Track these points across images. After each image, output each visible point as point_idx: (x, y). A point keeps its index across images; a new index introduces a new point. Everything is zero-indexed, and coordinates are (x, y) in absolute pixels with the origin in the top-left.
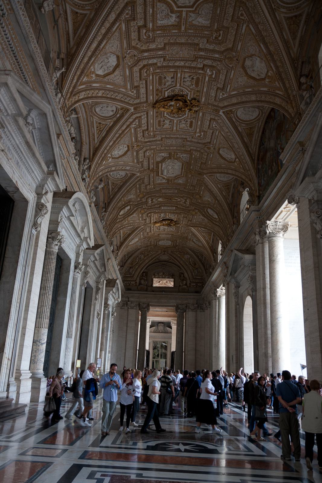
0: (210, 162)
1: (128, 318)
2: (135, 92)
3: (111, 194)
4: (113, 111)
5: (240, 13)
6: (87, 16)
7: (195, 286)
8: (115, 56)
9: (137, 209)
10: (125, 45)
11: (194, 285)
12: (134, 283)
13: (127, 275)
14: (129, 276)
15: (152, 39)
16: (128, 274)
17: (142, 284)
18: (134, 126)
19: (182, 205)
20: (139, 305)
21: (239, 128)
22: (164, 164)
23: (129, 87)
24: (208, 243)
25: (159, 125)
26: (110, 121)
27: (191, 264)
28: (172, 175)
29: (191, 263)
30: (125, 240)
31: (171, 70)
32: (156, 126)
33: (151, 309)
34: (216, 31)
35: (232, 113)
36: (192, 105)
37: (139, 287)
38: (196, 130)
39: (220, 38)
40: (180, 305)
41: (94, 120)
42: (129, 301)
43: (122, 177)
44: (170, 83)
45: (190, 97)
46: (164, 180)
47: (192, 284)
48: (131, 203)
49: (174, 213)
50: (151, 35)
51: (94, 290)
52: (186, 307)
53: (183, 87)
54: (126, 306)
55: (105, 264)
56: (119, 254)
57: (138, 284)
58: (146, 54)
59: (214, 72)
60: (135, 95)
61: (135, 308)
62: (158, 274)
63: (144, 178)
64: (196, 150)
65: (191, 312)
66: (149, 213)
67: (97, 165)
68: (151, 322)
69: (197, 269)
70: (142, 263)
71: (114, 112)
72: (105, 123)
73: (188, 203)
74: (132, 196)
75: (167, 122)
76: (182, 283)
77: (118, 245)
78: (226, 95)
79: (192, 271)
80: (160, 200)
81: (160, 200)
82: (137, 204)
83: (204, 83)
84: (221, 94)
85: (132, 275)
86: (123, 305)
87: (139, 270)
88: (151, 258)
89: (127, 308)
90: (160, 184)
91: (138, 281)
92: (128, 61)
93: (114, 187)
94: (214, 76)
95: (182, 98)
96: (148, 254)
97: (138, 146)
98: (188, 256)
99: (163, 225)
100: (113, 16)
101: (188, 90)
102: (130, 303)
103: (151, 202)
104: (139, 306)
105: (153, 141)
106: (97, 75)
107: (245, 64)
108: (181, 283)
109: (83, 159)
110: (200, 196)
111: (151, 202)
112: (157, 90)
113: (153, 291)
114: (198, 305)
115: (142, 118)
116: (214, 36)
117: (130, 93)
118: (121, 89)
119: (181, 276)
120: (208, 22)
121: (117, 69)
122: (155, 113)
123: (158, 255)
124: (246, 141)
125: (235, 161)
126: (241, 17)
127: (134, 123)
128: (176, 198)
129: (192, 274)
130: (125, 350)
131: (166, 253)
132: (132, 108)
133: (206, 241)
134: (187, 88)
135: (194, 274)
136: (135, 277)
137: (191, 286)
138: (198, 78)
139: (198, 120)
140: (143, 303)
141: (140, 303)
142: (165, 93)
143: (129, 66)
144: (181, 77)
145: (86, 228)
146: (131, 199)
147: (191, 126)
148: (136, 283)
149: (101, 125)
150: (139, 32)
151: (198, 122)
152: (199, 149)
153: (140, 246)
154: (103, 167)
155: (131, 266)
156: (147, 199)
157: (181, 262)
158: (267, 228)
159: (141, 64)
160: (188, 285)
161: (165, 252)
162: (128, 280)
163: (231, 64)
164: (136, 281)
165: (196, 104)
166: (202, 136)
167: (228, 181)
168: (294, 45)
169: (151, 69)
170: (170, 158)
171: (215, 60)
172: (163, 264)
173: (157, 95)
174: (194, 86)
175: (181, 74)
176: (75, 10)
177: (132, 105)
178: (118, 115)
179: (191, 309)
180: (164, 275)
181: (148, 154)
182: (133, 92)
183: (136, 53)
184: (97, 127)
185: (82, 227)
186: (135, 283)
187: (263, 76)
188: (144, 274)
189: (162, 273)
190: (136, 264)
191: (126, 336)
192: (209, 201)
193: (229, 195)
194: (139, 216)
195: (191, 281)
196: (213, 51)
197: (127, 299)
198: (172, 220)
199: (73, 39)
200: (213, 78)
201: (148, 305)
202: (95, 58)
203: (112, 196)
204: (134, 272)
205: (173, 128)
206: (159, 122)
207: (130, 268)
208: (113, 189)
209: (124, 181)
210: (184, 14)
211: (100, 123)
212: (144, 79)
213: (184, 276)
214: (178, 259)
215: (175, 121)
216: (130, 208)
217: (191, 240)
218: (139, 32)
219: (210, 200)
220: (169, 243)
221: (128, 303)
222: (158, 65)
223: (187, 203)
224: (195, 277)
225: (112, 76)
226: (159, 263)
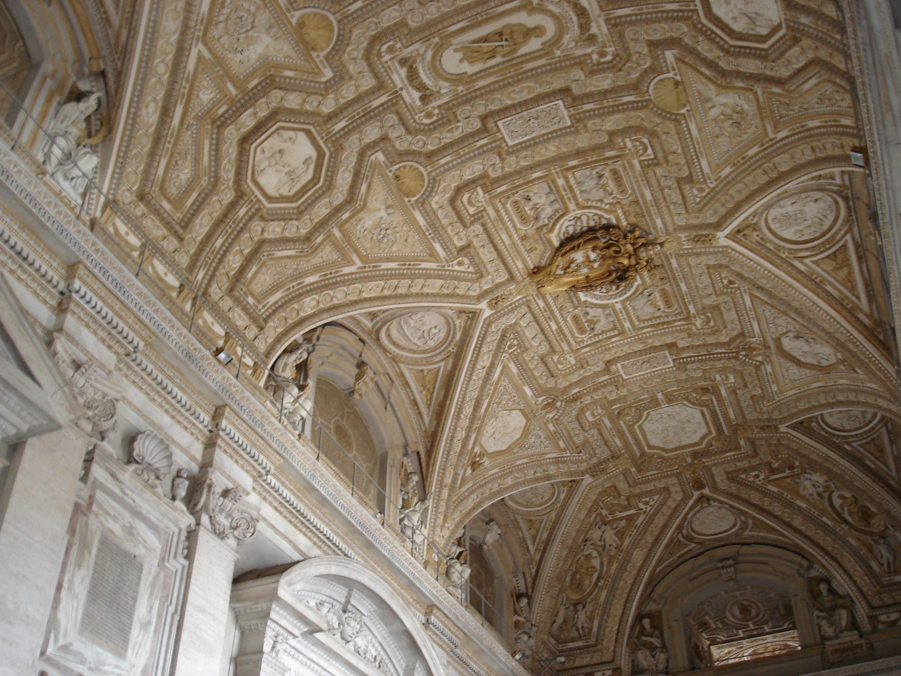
3: (115, 20)
9: (362, 155)
13: (571, 645)
14: (580, 644)
16: (573, 640)
19: (580, 62)
27: (846, 522)
29: (846, 516)
47: (883, 618)
66: (459, 190)
69: (883, 536)
70: (622, 569)
73: (605, 30)
76: (831, 624)
79: (864, 551)
85: (592, 640)
87: (617, 608)
88: (650, 538)
96: (630, 519)
98: (816, 477)
99: (589, 285)
108: (824, 623)
119: (820, 593)
123: (676, 510)
128: (524, 19)
129: (869, 567)
131: (706, 491)
133: (838, 304)
135: (874, 565)
136: (608, 643)
137: (881, 626)
157: (797, 522)
160: (866, 626)
162: (577, 664)
164: (612, 661)
172: (721, 560)
186: (615, 670)
189: (737, 612)
190: (596, 584)
195: (876, 602)
198: (608, 227)
204: (596, 623)
207: (575, 605)
213: (831, 591)
214: (777, 509)
217: (771, 344)
223: (594, 30)
224: (885, 580)
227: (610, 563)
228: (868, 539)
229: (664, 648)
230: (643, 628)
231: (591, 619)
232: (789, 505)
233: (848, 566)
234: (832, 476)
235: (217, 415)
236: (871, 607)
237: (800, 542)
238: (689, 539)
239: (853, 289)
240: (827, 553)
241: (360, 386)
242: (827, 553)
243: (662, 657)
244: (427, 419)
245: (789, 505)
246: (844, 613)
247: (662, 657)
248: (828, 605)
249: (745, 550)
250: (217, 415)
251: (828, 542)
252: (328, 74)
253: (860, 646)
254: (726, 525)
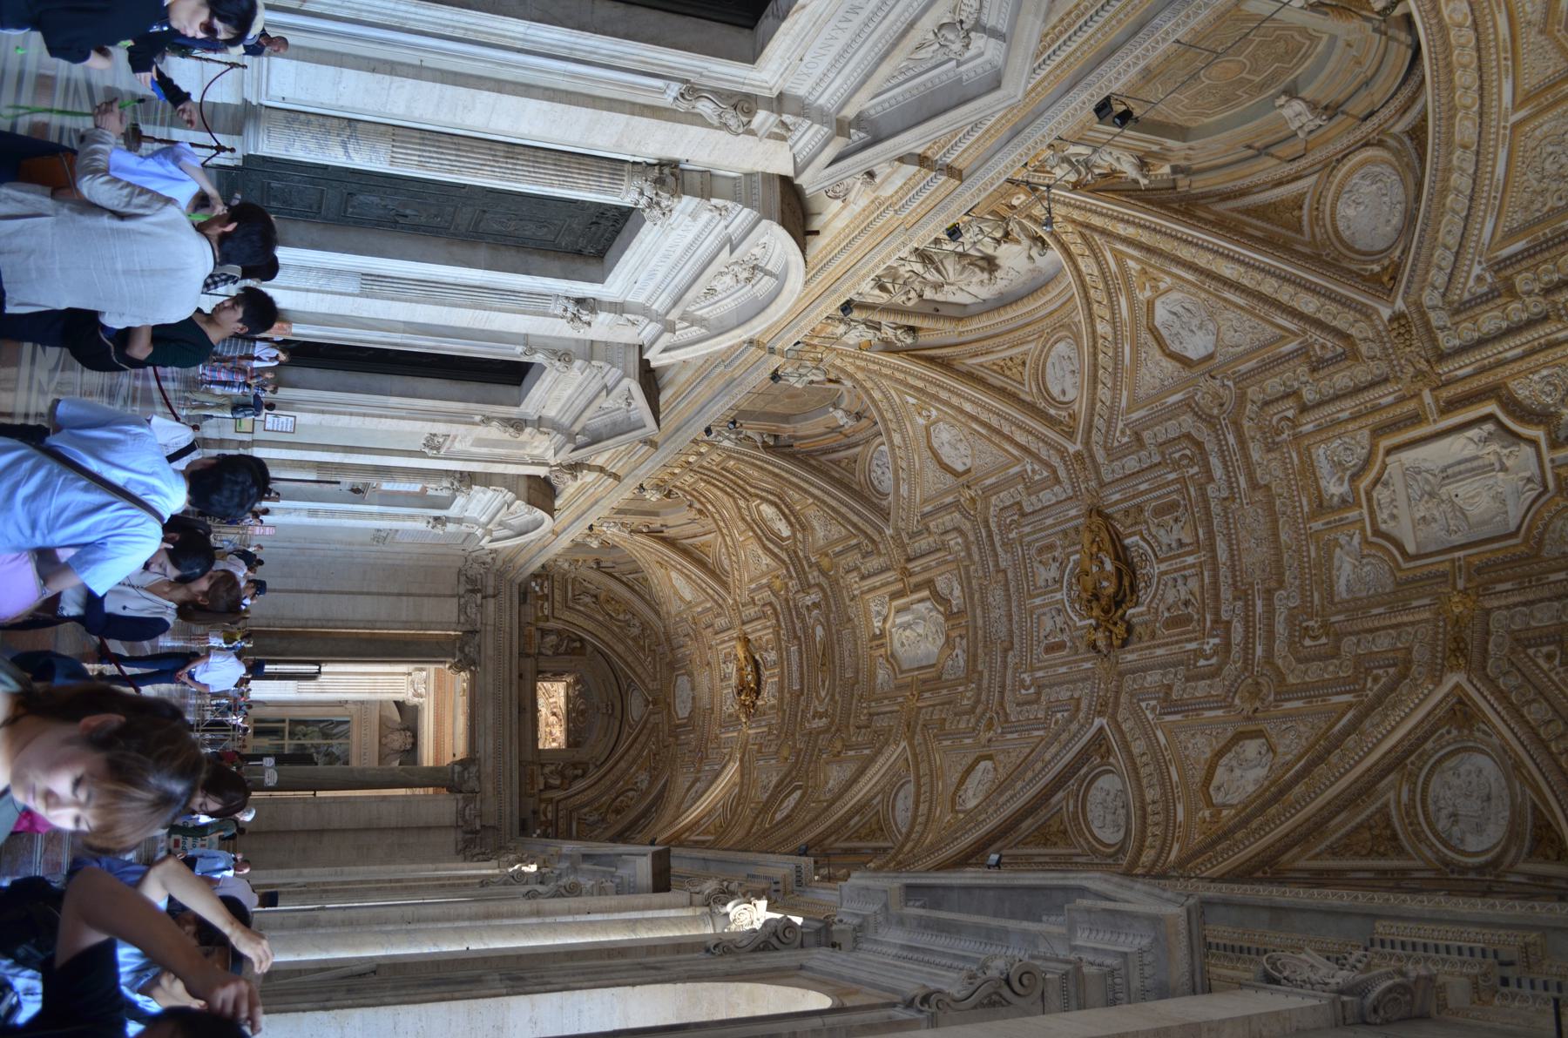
0: (948, 743)
1: (429, 596)
2: (1125, 440)
3: (823, 458)
4: (1064, 392)
5: (1381, 672)
6: (1299, 236)
7: (543, 818)
8: (1211, 349)
9: (783, 562)
10: (1244, 368)
11: (546, 816)
12: (546, 612)
13: (570, 588)
14: (570, 595)
15: (1274, 442)
16: (573, 590)
17: (542, 637)
18: (1029, 468)
20: (474, 632)
21: (1060, 794)
22: (928, 604)
23: (1135, 416)
24: (691, 827)
25: (1040, 551)
26: (1035, 390)
27: (617, 797)
28: (897, 644)
30: (685, 552)
31: (1201, 532)
32: (1037, 540)
33: (461, 680)
34: (1325, 626)
35: (1102, 757)
36: (1111, 627)
37: (533, 629)
38: (1040, 669)
39: (1308, 642)
40: (478, 771)
41: (1032, 345)
43: (876, 483)
44: (1165, 540)
45: (1133, 615)
46: (880, 624)
47: (550, 808)
48: (799, 536)
49: (781, 689)
50: (1284, 436)
51: (513, 412)
52: (473, 791)
53: (1158, 583)
54: (469, 587)
55: (599, 441)
56: (637, 537)
57: (541, 624)
58: (1231, 439)
59: (1214, 660)
60: (1116, 444)
61: (462, 619)
62: (580, 695)
63: (879, 554)
64: (979, 687)
66: (775, 609)
67: (901, 371)
68: (416, 700)
69: (603, 820)
71: (1062, 399)
72: (1026, 378)
74: (820, 533)
75: (1054, 572)
76: (551, 773)
77: (668, 533)
78: (1150, 717)
80: (819, 631)
81: (819, 631)
82: (797, 556)
83: (1177, 642)
84: (1153, 703)
85: (570, 604)
86: (469, 580)
87: (590, 626)
88: (629, 659)
89: (462, 591)
90: (867, 612)
91: (552, 624)
92: (1204, 390)
93: (843, 465)
94: (1202, 662)
95: (1128, 592)
96: (643, 648)
97: (973, 500)
99: (740, 670)
100: (1308, 304)
101: (1151, 602)
102: (479, 602)
103: (809, 603)
104: (471, 632)
105: (992, 544)
106: (1150, 305)
107: (1247, 742)
108: (553, 767)
109: (912, 322)
110: (839, 753)
111: (809, 603)
112: (1140, 509)
113: (521, 676)
114: (477, 832)
115: (1056, 488)
116: (1311, 623)
117: (1120, 425)
118: (1125, 393)
120: (1344, 595)
121: (1178, 365)
122: (1075, 523)
123: (643, 682)
124: (1024, 825)
125: (957, 812)
126: (1370, 679)
127: (1037, 467)
130: (320, 592)
132: (1079, 447)
133: (696, 823)
134: (1158, 597)
135: (587, 809)
136: (567, 615)
137: (543, 806)
138: (1189, 619)
139: (1069, 662)
140: (479, 646)
142: (1134, 534)
143: (1193, 397)
144: (1184, 568)
145: (703, 331)
146: (813, 529)
147: (1051, 649)
148: (547, 619)
149: (1020, 368)
150: (1286, 396)
151: (1063, 664)
152: (983, 697)
153: (668, 613)
154: (897, 400)
155: (602, 597)
156: (818, 585)
157: (623, 764)
158: (742, 900)
159: (1204, 434)
161: (655, 703)
163: (1241, 698)
165: (1114, 637)
166: (1023, 692)
167: (896, 825)
168: (1316, 857)
169: (1196, 469)
170: (949, 616)
171: (1247, 648)
173: (1127, 513)
174: (1166, 614)
175: (1193, 566)
176: (1307, 202)
177: (1087, 443)
178: (1052, 412)
179: (464, 809)
180: (576, 718)
181: (952, 543)
182: (1123, 433)
183: (1228, 407)
184: (1011, 359)
185: (705, 320)
187: (1217, 798)
188: (578, 644)
189: (582, 707)
191: (368, 593)
192: (827, 783)
193: (849, 839)
194: (763, 575)
195: (561, 806)
196: (1270, 635)
197: (490, 591)
198: (758, 693)
199: (1233, 210)
200: (1196, 661)
201: (474, 663)
202: (1193, 285)
203: (813, 462)
205: (1039, 595)
206: (1051, 547)
208: (837, 462)
209: (867, 493)
210: (1352, 514)
211: (1024, 363)
212: (1163, 454)
213: (576, 777)
214: (633, 752)
215: (1058, 596)
216: (783, 539)
218: (1286, 396)
219: (830, 786)
220: (682, 711)
221: (479, 595)
222: (1210, 488)
224: (575, 815)
225: (1157, 353)
226: (617, 693)
227: (619, 627)
228: (603, 810)
229: (556, 654)
230: (575, 641)
231: (585, 605)
232: (634, 761)
233: (589, 792)
234: (644, 794)
235: (616, 477)
236: (559, 801)
237: (611, 762)
238: (629, 686)
239: (703, 833)
240: (600, 780)
241: (694, 512)
242: (600, 780)
243: (550, 653)
244: (684, 541)
245: (634, 761)
246: (558, 782)
247: (550, 653)
248: (566, 772)
249: (617, 724)
250: (616, 477)
251: (607, 782)
252: (813, 560)
253: (533, 788)
254: (634, 715)
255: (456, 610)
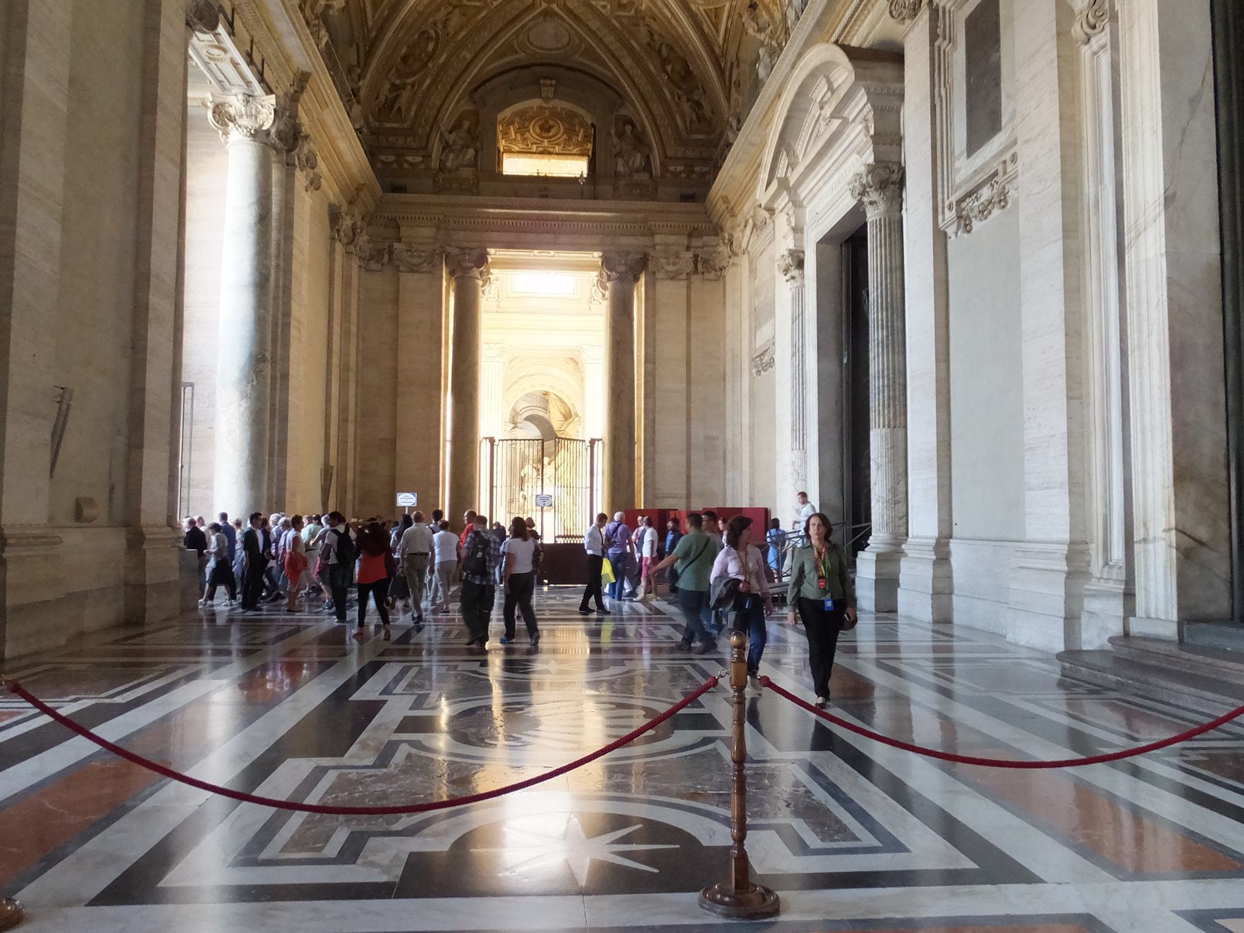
11: (680, 172)
42: (399, 240)
47: (672, 168)
61: (426, 267)
65: (667, 282)
119: (624, 132)
141: (449, 249)
179: (667, 272)
195: (670, 153)
221: (396, 245)
236: (666, 157)
255: (417, 276)
